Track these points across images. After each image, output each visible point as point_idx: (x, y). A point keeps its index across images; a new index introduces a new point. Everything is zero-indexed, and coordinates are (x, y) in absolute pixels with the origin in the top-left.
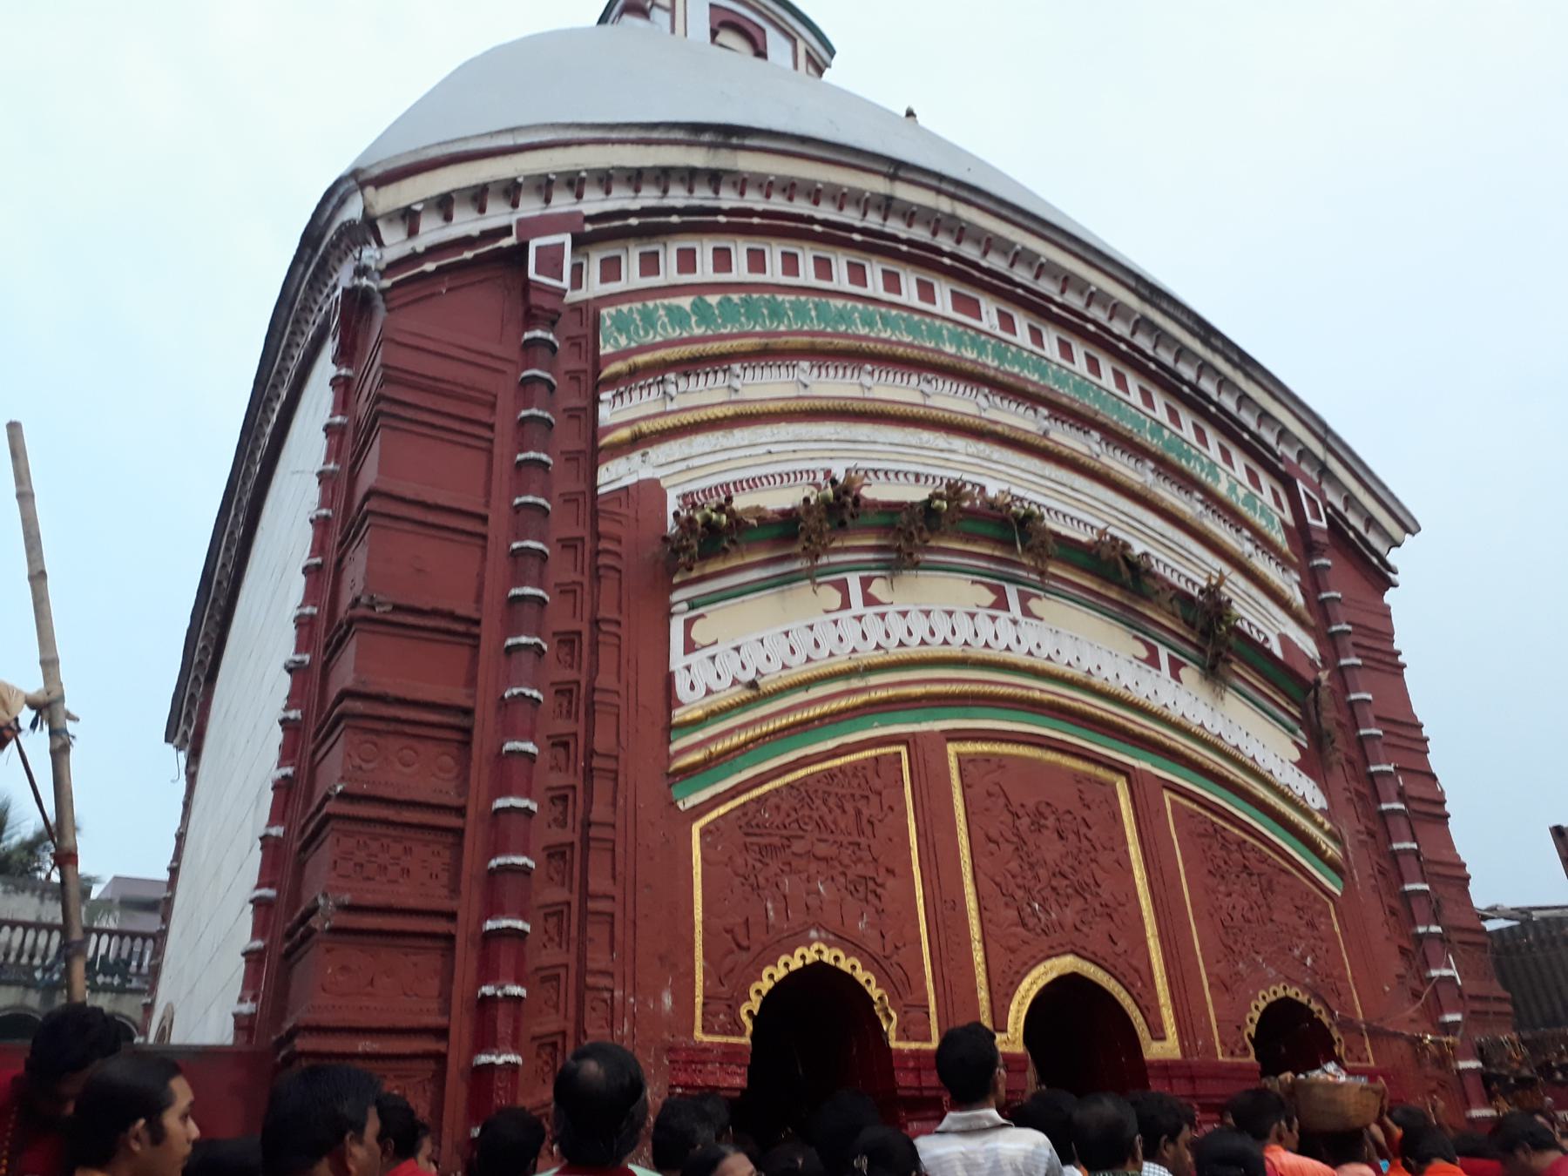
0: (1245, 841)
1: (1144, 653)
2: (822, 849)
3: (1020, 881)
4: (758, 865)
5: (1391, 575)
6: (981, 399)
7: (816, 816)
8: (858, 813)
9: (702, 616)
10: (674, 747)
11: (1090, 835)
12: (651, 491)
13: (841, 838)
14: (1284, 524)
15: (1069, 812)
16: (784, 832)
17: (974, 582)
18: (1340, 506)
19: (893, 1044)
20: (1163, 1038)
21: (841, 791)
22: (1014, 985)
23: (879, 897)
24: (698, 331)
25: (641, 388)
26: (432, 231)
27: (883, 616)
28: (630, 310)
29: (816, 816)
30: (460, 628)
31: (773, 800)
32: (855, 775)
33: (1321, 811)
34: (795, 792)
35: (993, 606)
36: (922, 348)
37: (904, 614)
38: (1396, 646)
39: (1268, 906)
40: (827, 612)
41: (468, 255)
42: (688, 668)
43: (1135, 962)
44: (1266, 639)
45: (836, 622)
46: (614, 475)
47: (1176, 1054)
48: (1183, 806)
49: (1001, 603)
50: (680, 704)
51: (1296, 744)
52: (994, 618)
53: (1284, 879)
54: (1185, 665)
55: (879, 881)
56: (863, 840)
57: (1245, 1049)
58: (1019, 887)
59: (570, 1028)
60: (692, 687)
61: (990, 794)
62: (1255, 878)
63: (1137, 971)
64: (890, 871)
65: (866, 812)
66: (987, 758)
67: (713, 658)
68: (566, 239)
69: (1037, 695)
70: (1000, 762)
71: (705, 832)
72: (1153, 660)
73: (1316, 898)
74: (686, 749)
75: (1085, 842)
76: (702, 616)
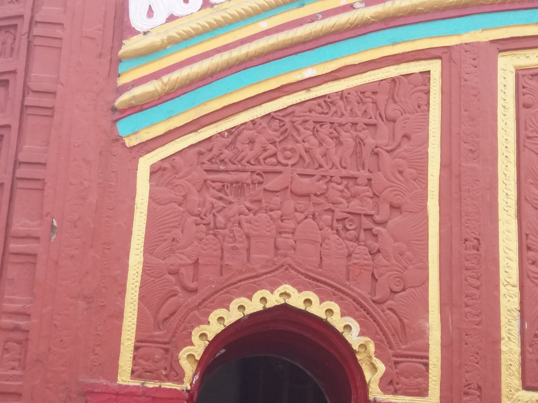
2: (305, 184)
4: (221, 204)
8: (360, 142)
13: (333, 172)
16: (258, 168)
21: (336, 119)
23: (375, 236)
29: (300, 147)
32: (361, 102)
34: (276, 124)
55: (377, 218)
56: (363, 174)
64: (395, 208)
65: (370, 141)
71: (156, 171)
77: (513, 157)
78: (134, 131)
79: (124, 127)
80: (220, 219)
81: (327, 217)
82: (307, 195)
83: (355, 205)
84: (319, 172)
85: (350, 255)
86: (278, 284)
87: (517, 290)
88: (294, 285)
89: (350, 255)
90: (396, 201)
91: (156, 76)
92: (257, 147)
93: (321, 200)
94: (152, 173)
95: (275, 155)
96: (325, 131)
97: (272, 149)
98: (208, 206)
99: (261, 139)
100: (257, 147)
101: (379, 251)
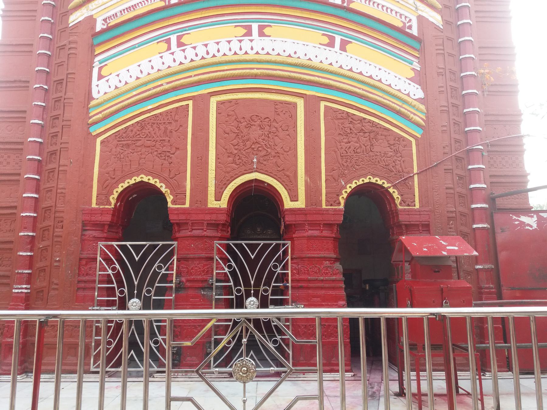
0: (365, 119)
1: (326, 40)
3: (236, 147)
7: (147, 131)
9: (106, 65)
10: (90, 115)
11: (276, 125)
12: (91, 20)
16: (134, 139)
17: (236, 26)
19: (170, 205)
20: (297, 201)
21: (159, 122)
22: (226, 185)
27: (184, 51)
29: (147, 131)
30: (23, 85)
31: (130, 128)
33: (419, 100)
35: (245, 35)
37: (194, 48)
39: (372, 145)
40: (159, 53)
42: (97, 86)
43: (288, 173)
45: (161, 57)
46: (75, 18)
47: (303, 206)
49: (249, 33)
51: (413, 69)
52: (240, 41)
53: (385, 133)
54: (351, 42)
55: (171, 152)
57: (339, 204)
58: (236, 149)
59: (53, 204)
60: (99, 92)
62: (367, 134)
63: (288, 176)
64: (177, 149)
65: (169, 128)
66: (230, 101)
67: (107, 81)
69: (255, 71)
70: (237, 102)
71: (102, 142)
73: (404, 139)
74: (95, 113)
75: (274, 129)
76: (106, 65)
77: (215, 130)
78: (95, 130)
79: (91, 129)
80: (122, 156)
83: (165, 149)
84: (153, 139)
90: (177, 147)
91: (100, 112)
92: (134, 132)
93: (154, 148)
96: (155, 125)
97: (138, 133)
98: (118, 152)
99: (135, 130)
100: (134, 132)
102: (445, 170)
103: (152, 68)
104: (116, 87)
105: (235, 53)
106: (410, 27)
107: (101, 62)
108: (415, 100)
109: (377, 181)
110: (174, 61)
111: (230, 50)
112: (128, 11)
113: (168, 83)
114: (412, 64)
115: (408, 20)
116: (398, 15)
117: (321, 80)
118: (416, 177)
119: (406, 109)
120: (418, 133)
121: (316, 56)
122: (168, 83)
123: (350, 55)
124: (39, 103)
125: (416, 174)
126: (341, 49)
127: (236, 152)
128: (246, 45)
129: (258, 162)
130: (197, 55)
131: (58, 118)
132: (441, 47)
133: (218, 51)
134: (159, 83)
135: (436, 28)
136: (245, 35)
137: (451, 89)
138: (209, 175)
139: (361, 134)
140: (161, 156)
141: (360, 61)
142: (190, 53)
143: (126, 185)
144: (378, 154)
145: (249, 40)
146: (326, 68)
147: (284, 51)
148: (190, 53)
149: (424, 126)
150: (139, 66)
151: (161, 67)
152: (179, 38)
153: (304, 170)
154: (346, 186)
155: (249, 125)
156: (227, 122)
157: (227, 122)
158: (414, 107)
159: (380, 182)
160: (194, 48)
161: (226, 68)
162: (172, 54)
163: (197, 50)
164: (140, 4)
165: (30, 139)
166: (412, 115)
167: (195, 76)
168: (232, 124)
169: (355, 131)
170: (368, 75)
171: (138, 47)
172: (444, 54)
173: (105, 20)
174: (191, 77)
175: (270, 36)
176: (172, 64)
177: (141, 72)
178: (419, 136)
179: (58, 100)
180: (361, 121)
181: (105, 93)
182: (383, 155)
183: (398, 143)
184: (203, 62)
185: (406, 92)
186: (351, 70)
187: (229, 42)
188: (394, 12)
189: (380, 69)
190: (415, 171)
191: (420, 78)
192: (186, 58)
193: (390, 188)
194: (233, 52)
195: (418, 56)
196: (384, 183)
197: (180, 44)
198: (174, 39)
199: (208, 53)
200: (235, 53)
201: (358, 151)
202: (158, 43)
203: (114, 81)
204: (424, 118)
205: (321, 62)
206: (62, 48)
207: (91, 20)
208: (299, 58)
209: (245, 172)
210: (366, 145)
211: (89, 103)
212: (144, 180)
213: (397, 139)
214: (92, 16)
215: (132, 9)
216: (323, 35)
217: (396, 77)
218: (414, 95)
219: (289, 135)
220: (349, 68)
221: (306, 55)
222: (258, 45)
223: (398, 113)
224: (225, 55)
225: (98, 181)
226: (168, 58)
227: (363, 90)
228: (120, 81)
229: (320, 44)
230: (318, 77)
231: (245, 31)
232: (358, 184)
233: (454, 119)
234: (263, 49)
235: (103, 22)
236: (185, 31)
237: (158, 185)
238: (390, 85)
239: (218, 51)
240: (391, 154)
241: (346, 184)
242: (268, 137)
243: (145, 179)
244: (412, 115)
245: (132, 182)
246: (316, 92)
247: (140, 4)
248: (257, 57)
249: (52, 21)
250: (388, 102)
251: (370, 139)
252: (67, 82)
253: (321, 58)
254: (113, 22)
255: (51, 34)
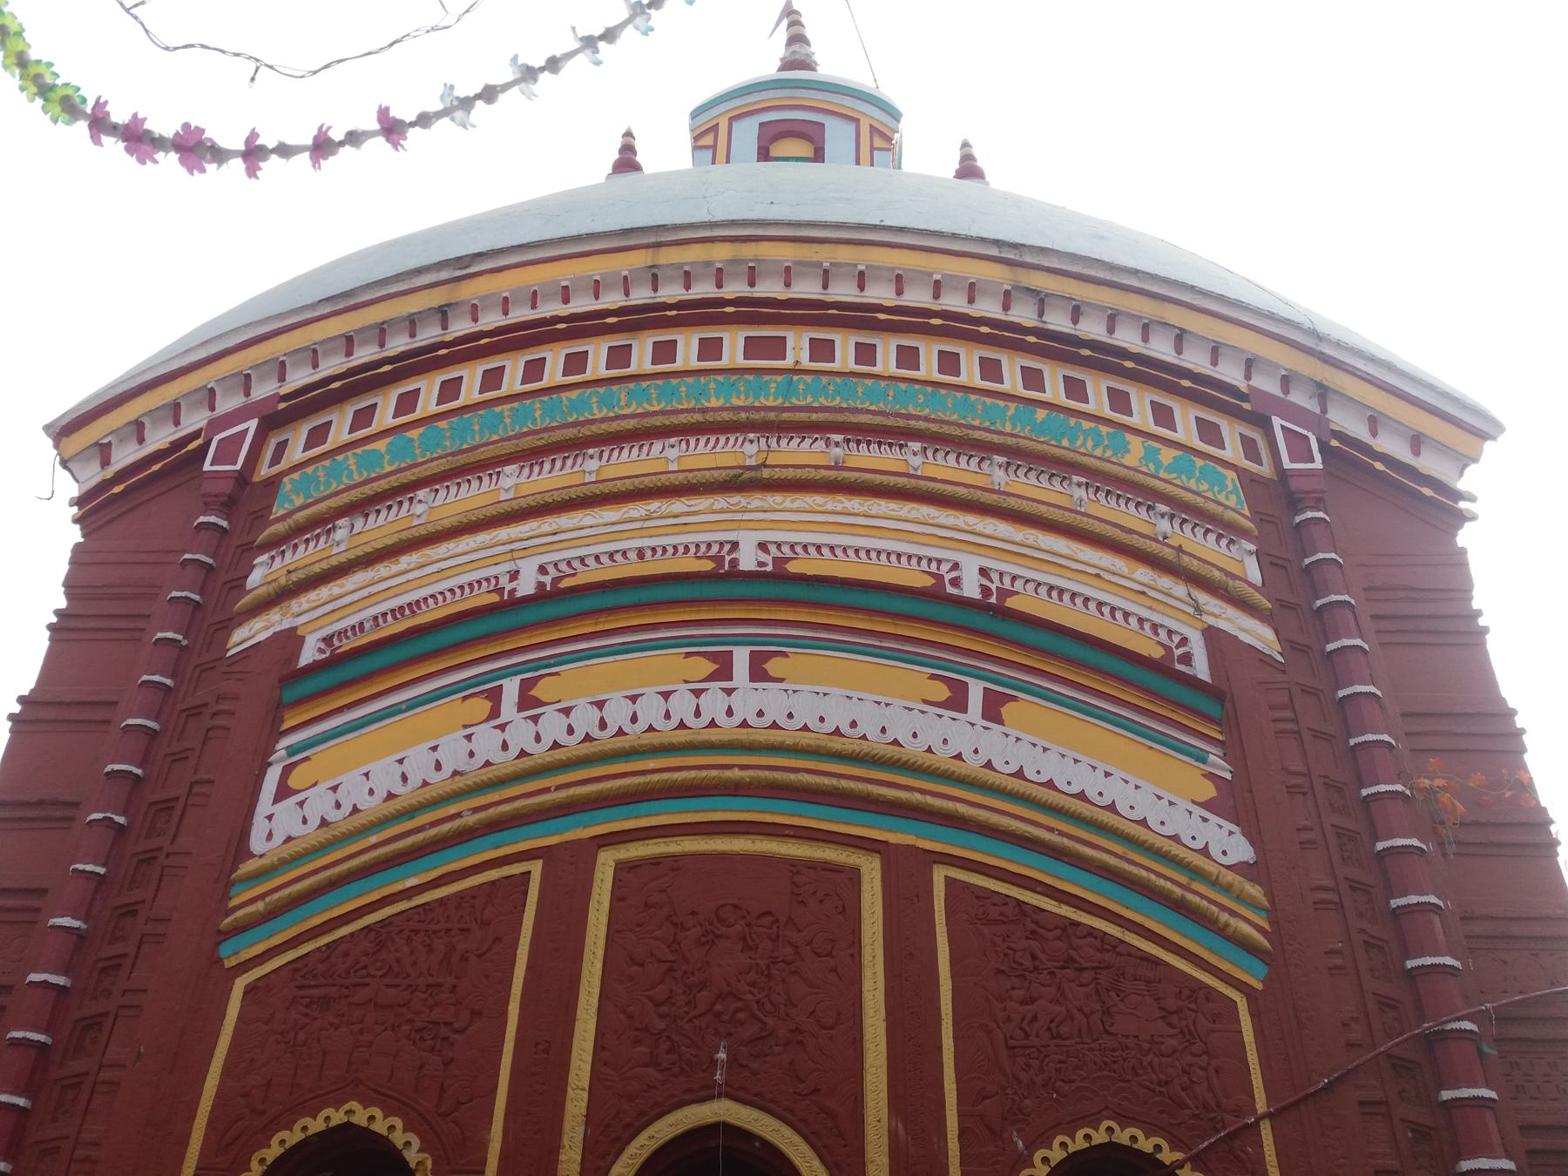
0: (1076, 924)
1: (942, 692)
5: (1462, 505)
6: (747, 444)
10: (234, 902)
12: (291, 640)
14: (1249, 481)
15: (769, 913)
16: (347, 982)
17: (689, 655)
18: (1357, 429)
21: (432, 926)
24: (388, 469)
25: (307, 541)
26: (125, 455)
27: (535, 719)
28: (316, 470)
30: (59, 813)
36: (704, 411)
38: (1475, 605)
39: (1107, 1012)
40: (465, 727)
41: (156, 468)
42: (270, 818)
44: (1184, 641)
45: (469, 737)
46: (249, 634)
48: (967, 886)
49: (724, 670)
50: (252, 856)
51: (1211, 776)
52: (698, 693)
54: (1014, 698)
55: (456, 1026)
58: (662, 1017)
60: (270, 836)
61: (647, 905)
62: (1087, 976)
66: (655, 861)
67: (301, 804)
68: (253, 424)
69: (737, 774)
71: (249, 990)
72: (957, 701)
75: (789, 950)
77: (600, 953)
80: (301, 1036)
81: (406, 1028)
82: (391, 1006)
85: (421, 1067)
86: (345, 1102)
87: (585, 1095)
88: (360, 1102)
89: (421, 1067)
91: (262, 897)
94: (245, 993)
95: (365, 967)
97: (364, 960)
101: (452, 1060)
102: (1361, 1103)
103: (438, 767)
104: (324, 823)
105: (682, 725)
106: (1187, 659)
107: (292, 750)
108: (1228, 867)
109: (1134, 1138)
110: (505, 746)
111: (667, 716)
112: (395, 618)
113: (475, 810)
114: (1204, 761)
115: (1176, 639)
116: (1147, 626)
117: (929, 799)
118: (1266, 1130)
119: (1202, 897)
120: (1253, 974)
121: (915, 735)
122: (475, 810)
123: (1015, 733)
124: (89, 868)
125: (1263, 1117)
126: (985, 716)
127: (661, 1025)
128: (714, 702)
129: (733, 1061)
130: (570, 730)
131: (134, 913)
132: (1289, 714)
133: (634, 719)
134: (452, 810)
135: (1263, 659)
136: (711, 678)
137: (1339, 835)
138: (569, 1105)
139: (1069, 973)
140: (423, 1039)
141: (1045, 749)
142: (552, 725)
143: (293, 1137)
144: (1131, 1042)
145: (723, 690)
146: (943, 767)
147: (822, 719)
148: (552, 725)
149: (1266, 951)
150: (401, 761)
151: (463, 763)
152: (526, 686)
153: (884, 1095)
154: (1031, 1156)
155: (710, 937)
156: (640, 925)
157: (640, 925)
158: (1227, 889)
159: (1146, 1145)
160: (567, 711)
161: (651, 764)
162: (502, 727)
163: (574, 718)
164: (431, 601)
165: (35, 977)
166: (1224, 917)
167: (558, 788)
168: (657, 933)
169: (1049, 964)
170: (1074, 789)
171: (408, 709)
172: (1298, 732)
173: (328, 640)
174: (546, 790)
175: (781, 680)
176: (498, 757)
177: (404, 778)
178: (1259, 986)
179: (147, 859)
180: (1064, 929)
181: (289, 839)
182: (1146, 1046)
183: (1193, 1007)
184: (588, 749)
185: (1199, 845)
186: (1019, 774)
187: (666, 695)
188: (1133, 621)
189: (1107, 774)
190: (1261, 1105)
191: (1230, 802)
192: (538, 738)
193: (1181, 1167)
194: (674, 722)
195: (1220, 737)
196: (1158, 1148)
197: (527, 701)
198: (511, 688)
199: (603, 725)
200: (682, 725)
201: (1064, 1029)
202: (465, 698)
203: (319, 804)
204: (1266, 926)
205: (929, 750)
206: (195, 712)
207: (291, 640)
208: (864, 737)
209: (687, 1097)
210: (1087, 1010)
211: (234, 868)
212: (355, 1120)
213: (1186, 993)
214: (293, 629)
215: (407, 612)
216: (933, 677)
217: (1160, 798)
218: (1224, 853)
219: (834, 970)
220: (1013, 768)
221: (883, 730)
222: (748, 703)
223: (1180, 907)
224: (651, 729)
225: (209, 1124)
226: (487, 741)
227: (1061, 833)
228: (338, 805)
229: (926, 702)
230: (922, 791)
231: (711, 667)
232: (1071, 1149)
233: (1364, 931)
234: (760, 714)
235: (322, 646)
236: (546, 667)
237: (398, 1138)
238: (1143, 823)
239: (634, 719)
240: (1173, 1042)
241: (1032, 1147)
242: (769, 976)
243: (360, 1118)
244: (1224, 917)
245: (316, 1125)
246: (918, 837)
247: (431, 601)
248: (742, 735)
249: (185, 643)
250: (1144, 873)
251: (1097, 992)
252: (186, 805)
253: (931, 737)
254: (347, 645)
255: (173, 676)
